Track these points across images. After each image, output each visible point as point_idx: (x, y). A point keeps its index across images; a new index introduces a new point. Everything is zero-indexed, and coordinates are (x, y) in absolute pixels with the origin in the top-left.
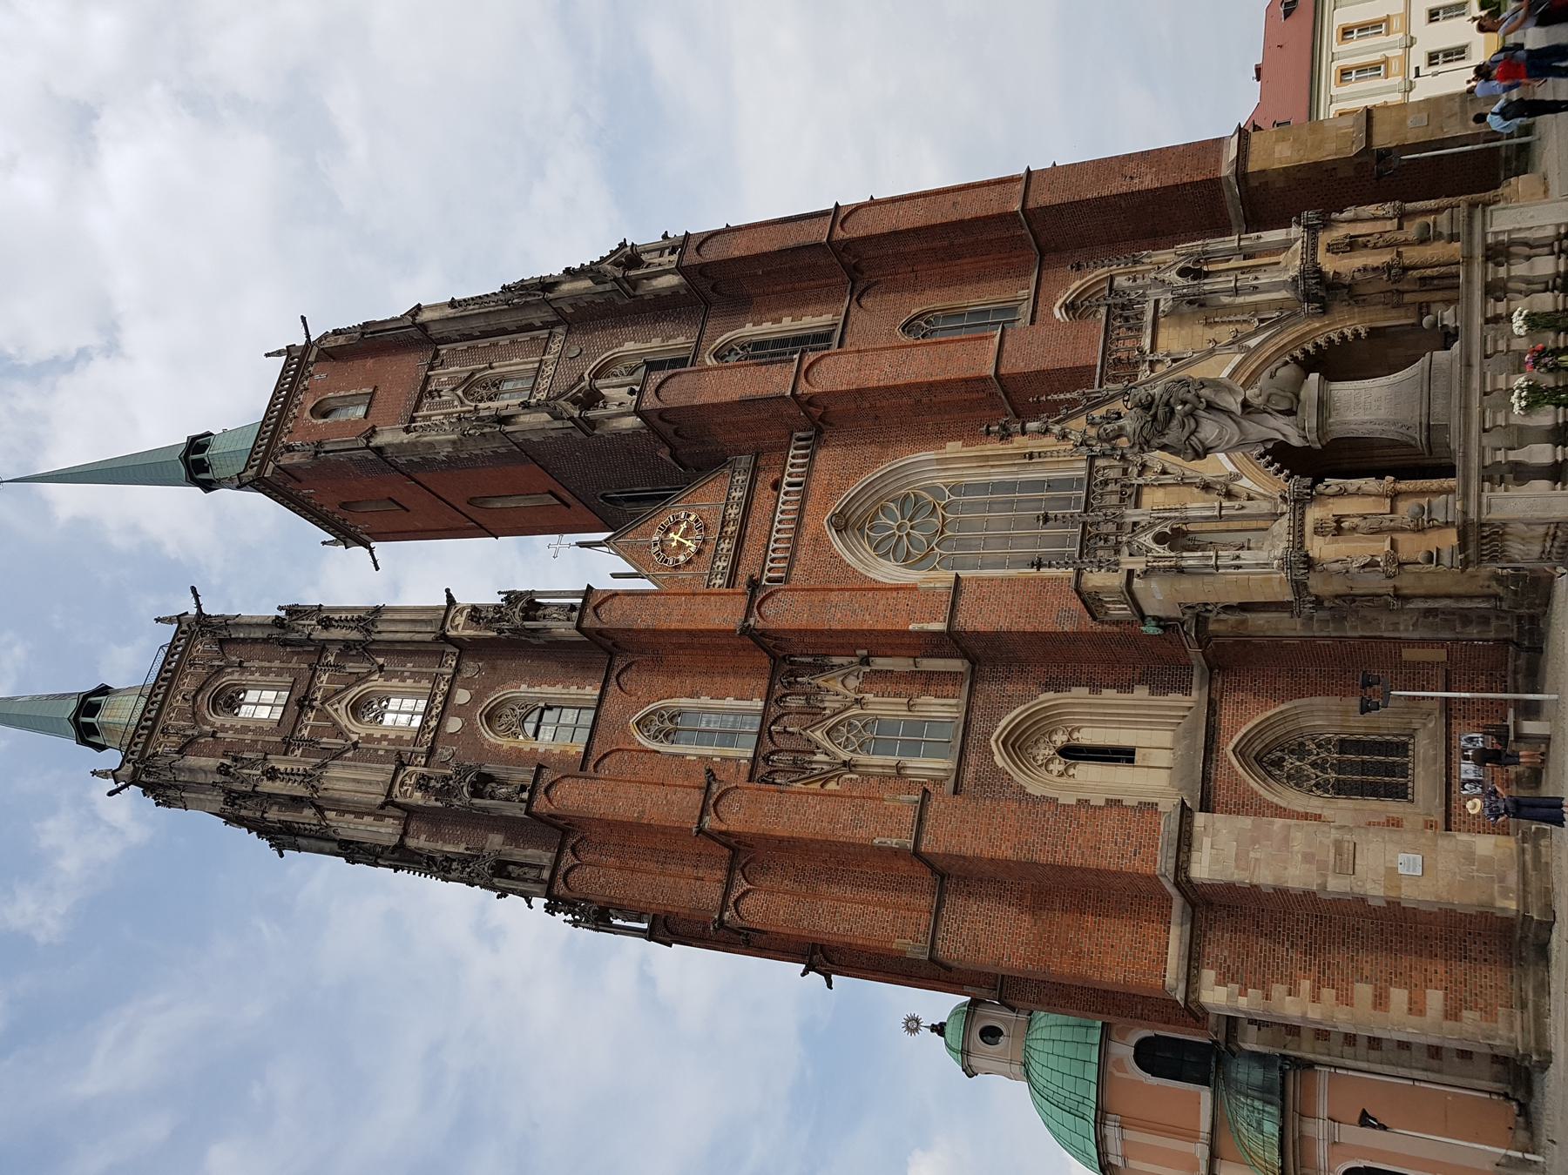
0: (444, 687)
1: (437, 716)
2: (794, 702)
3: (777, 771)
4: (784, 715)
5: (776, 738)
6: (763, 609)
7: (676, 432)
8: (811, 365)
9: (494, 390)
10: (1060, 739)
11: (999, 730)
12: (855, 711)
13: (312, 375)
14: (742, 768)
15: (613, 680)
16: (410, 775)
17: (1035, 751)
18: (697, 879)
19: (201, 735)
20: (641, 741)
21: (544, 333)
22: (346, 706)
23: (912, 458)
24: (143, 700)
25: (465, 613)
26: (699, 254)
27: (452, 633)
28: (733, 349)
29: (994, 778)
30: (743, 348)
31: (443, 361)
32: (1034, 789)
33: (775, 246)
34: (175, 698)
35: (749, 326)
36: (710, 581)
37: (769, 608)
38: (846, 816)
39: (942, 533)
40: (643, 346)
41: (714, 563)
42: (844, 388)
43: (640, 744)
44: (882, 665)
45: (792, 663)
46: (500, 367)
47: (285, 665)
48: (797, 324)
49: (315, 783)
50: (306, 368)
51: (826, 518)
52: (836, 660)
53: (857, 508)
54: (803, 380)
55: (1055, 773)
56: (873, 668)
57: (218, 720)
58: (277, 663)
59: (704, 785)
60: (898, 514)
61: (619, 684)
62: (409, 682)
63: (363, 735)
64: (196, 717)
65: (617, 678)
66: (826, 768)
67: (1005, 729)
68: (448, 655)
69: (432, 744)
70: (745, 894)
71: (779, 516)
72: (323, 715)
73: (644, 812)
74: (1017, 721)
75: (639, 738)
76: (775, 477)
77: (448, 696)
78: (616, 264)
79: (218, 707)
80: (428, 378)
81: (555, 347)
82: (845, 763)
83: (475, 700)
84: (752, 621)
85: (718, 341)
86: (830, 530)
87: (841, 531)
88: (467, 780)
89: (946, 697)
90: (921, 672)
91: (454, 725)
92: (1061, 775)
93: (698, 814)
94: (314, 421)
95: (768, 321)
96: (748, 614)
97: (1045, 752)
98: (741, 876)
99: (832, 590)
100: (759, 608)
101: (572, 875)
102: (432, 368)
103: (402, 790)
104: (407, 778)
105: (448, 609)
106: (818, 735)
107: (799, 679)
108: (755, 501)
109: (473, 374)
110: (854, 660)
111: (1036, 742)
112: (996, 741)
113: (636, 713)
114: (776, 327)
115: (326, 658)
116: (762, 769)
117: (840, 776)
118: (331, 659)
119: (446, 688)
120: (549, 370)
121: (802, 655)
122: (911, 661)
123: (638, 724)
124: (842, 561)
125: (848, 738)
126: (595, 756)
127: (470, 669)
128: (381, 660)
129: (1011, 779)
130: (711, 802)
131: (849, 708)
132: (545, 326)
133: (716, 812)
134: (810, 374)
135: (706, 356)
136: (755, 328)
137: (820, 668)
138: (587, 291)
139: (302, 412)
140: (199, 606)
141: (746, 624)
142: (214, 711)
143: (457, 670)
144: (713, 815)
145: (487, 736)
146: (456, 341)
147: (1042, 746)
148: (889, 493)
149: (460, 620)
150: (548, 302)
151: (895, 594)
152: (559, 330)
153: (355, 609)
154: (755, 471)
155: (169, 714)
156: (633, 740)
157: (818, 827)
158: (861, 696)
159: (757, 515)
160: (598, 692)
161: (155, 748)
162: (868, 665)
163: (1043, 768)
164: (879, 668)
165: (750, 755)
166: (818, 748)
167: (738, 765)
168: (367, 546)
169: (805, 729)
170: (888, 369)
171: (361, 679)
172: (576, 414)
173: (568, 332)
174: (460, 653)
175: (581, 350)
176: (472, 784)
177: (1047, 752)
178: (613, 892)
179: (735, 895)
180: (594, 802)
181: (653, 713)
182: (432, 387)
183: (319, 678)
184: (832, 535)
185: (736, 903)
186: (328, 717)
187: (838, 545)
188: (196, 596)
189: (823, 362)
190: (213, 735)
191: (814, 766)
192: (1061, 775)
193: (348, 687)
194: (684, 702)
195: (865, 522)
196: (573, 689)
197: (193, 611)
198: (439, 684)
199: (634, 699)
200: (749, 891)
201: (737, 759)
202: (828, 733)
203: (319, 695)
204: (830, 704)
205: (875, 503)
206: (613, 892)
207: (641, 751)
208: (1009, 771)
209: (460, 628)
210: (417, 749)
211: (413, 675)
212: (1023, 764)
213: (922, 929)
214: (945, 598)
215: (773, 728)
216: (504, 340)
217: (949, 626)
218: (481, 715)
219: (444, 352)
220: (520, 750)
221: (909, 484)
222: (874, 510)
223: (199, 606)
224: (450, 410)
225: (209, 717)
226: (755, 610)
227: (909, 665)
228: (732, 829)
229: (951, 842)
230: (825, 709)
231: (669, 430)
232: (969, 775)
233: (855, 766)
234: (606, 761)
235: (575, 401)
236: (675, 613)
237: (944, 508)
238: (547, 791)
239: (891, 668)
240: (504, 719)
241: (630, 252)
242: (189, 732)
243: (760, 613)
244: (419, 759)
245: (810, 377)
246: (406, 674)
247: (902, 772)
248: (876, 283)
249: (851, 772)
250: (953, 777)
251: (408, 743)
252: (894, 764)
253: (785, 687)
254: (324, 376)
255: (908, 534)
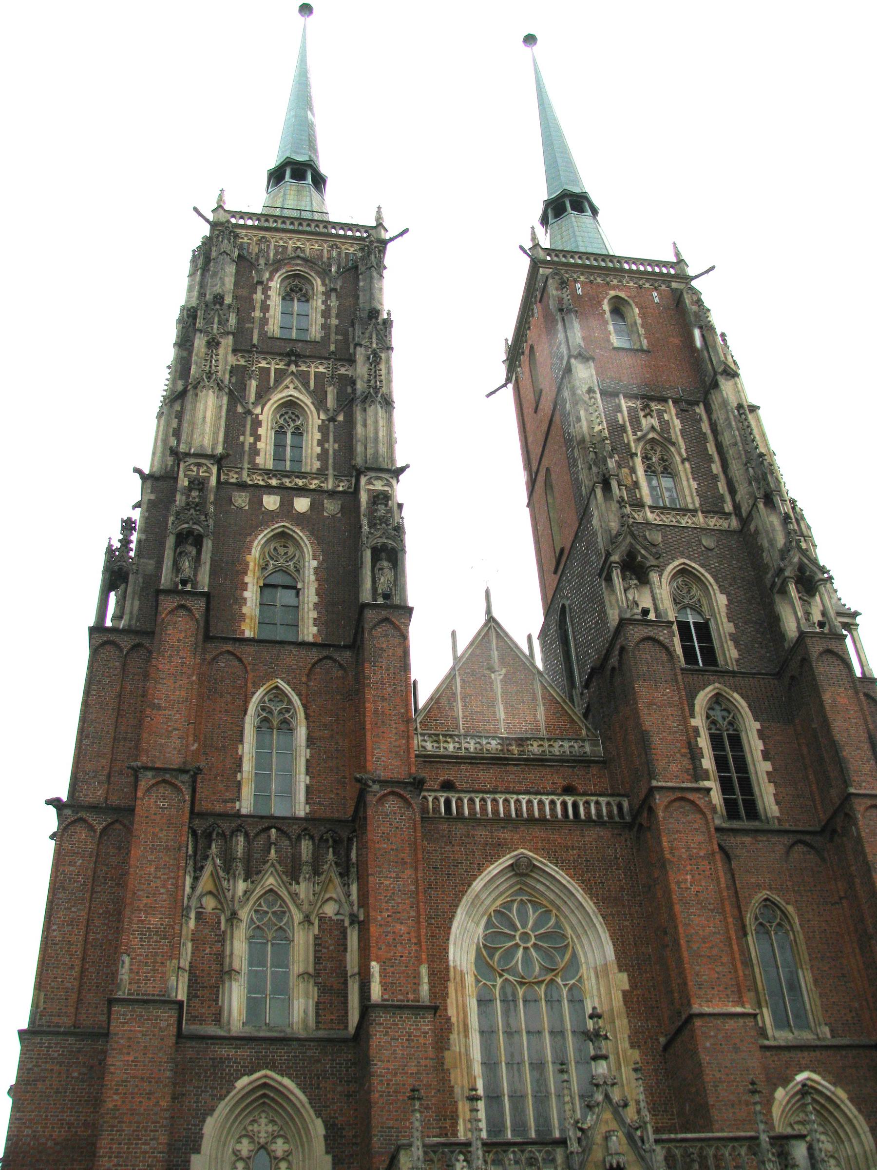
0: (314, 484)
1: (282, 484)
2: (306, 848)
3: (226, 842)
4: (290, 839)
5: (263, 836)
6: (391, 798)
7: (613, 669)
8: (692, 802)
9: (659, 469)
10: (279, 1147)
11: (278, 1078)
12: (297, 916)
13: (656, 289)
14: (229, 805)
15: (325, 653)
16: (208, 471)
17: (263, 1121)
18: (109, 776)
19: (259, 272)
20: (258, 694)
21: (728, 507)
22: (291, 396)
23: (605, 937)
24: (295, 214)
25: (386, 488)
26: (821, 654)
27: (363, 480)
28: (729, 713)
29: (221, 1078)
30: (731, 723)
31: (687, 411)
32: (210, 1126)
33: (839, 735)
34: (298, 240)
35: (757, 725)
36: (451, 736)
37: (391, 805)
38: (154, 920)
39: (522, 984)
40: (723, 614)
41: (472, 737)
42: (665, 844)
43: (254, 693)
44: (352, 941)
45: (350, 840)
46: (685, 470)
47: (333, 329)
48: (763, 778)
49: (202, 384)
50: (664, 282)
51: (526, 852)
52: (354, 888)
53: (544, 884)
54: (673, 796)
55: (238, 1147)
56: (349, 931)
57: (275, 284)
58: (334, 321)
59: (187, 768)
60: (542, 931)
61: (320, 660)
62: (318, 450)
63: (261, 417)
64: (276, 265)
65: (326, 658)
66: (229, 895)
67: (280, 1083)
68: (348, 481)
69: (251, 486)
70: (91, 828)
71: (524, 799)
72: (281, 375)
73: (159, 708)
74: (291, 1097)
75: (260, 692)
76: (579, 787)
77: (302, 491)
78: (801, 568)
79: (290, 280)
80: (664, 400)
81: (713, 522)
82: (234, 914)
83: (300, 519)
84: (376, 787)
85: (736, 695)
86: (511, 858)
87: (513, 870)
88: (195, 527)
89: (317, 1015)
90: (345, 983)
91: (271, 502)
92: (235, 1153)
93: (157, 765)
94: (606, 301)
95: (765, 744)
96: (383, 783)
97: (263, 1128)
98: (110, 820)
99: (416, 869)
100: (393, 793)
101: (112, 649)
102: (675, 402)
103: (192, 467)
104: (205, 468)
105: (388, 471)
106: (270, 881)
107: (331, 850)
108: (548, 770)
109: (673, 444)
110: (355, 908)
111: (272, 1121)
112: (266, 1076)
113: (288, 684)
114: (758, 755)
115: (343, 366)
116: (226, 826)
117: (223, 911)
118: (342, 371)
119: (312, 487)
120: (686, 521)
121: (357, 849)
122: (356, 970)
123: (277, 687)
124: (475, 877)
125: (267, 913)
126: (238, 649)
127: (331, 507)
128: (341, 418)
129: (222, 1098)
130: (167, 777)
131: (298, 906)
132: (737, 507)
133: (158, 783)
134: (683, 803)
135: (717, 685)
136: (755, 733)
137: (344, 874)
138: (772, 542)
139: (614, 288)
140: (392, 239)
141: (370, 783)
142: (288, 277)
143: (332, 494)
144: (154, 781)
145: (260, 537)
146: (710, 419)
147: (270, 1128)
148: (566, 917)
149: (378, 486)
150: (755, 505)
151: (414, 940)
152: (734, 523)
153: (389, 381)
154: (581, 762)
155: (281, 239)
156: (257, 686)
157: (140, 893)
158: (316, 923)
159: (533, 775)
160: (310, 639)
161: (246, 235)
162: (351, 923)
163: (244, 1133)
164: (349, 938)
165: (244, 811)
166: (252, 882)
167: (233, 801)
168: (508, 380)
169: (273, 865)
170: (693, 890)
171: (320, 403)
172: (615, 558)
173: (734, 532)
174: (351, 493)
175: (711, 550)
176: (190, 532)
177: (263, 1134)
178: (94, 693)
179: (91, 818)
180: (171, 656)
181: (290, 702)
182: (654, 406)
183: (321, 364)
184: (506, 861)
185: (81, 820)
186: (278, 381)
187: (494, 869)
188: (401, 234)
189: (698, 816)
190: (260, 283)
191: (231, 882)
192: (235, 1153)
193: (312, 394)
194: (302, 732)
195: (531, 895)
196: (314, 614)
197: (387, 236)
198: (315, 478)
199: (304, 679)
200: (95, 831)
201: (239, 799)
202: (271, 890)
203: (304, 368)
204: (303, 889)
205: (552, 902)
206: (94, 693)
207: (246, 696)
208: (232, 1094)
209: (367, 487)
210: (245, 474)
211: (325, 452)
212: (243, 1110)
213: (55, 1020)
214: (411, 996)
215: (273, 831)
216: (716, 468)
217: (377, 1006)
218: (284, 526)
219: (698, 411)
220: (246, 573)
221: (578, 937)
222: (545, 903)
223: (392, 239)
224: (629, 429)
225: (278, 274)
226: (389, 790)
227: (352, 968)
228: (139, 802)
229: (122, 1038)
230: (298, 883)
231: (614, 661)
232: (225, 1051)
233: (232, 925)
234: (237, 663)
235: (631, 555)
236: (384, 704)
237: (552, 980)
238: (182, 606)
239: (349, 950)
240: (282, 551)
241: (817, 578)
242: (262, 261)
243: (385, 795)
244: (236, 476)
245: (677, 804)
246: (326, 446)
247: (226, 977)
248: (823, 860)
249: (227, 921)
250: (222, 1033)
251: (252, 462)
252: (236, 965)
253: (322, 837)
254: (657, 300)
255: (517, 946)
